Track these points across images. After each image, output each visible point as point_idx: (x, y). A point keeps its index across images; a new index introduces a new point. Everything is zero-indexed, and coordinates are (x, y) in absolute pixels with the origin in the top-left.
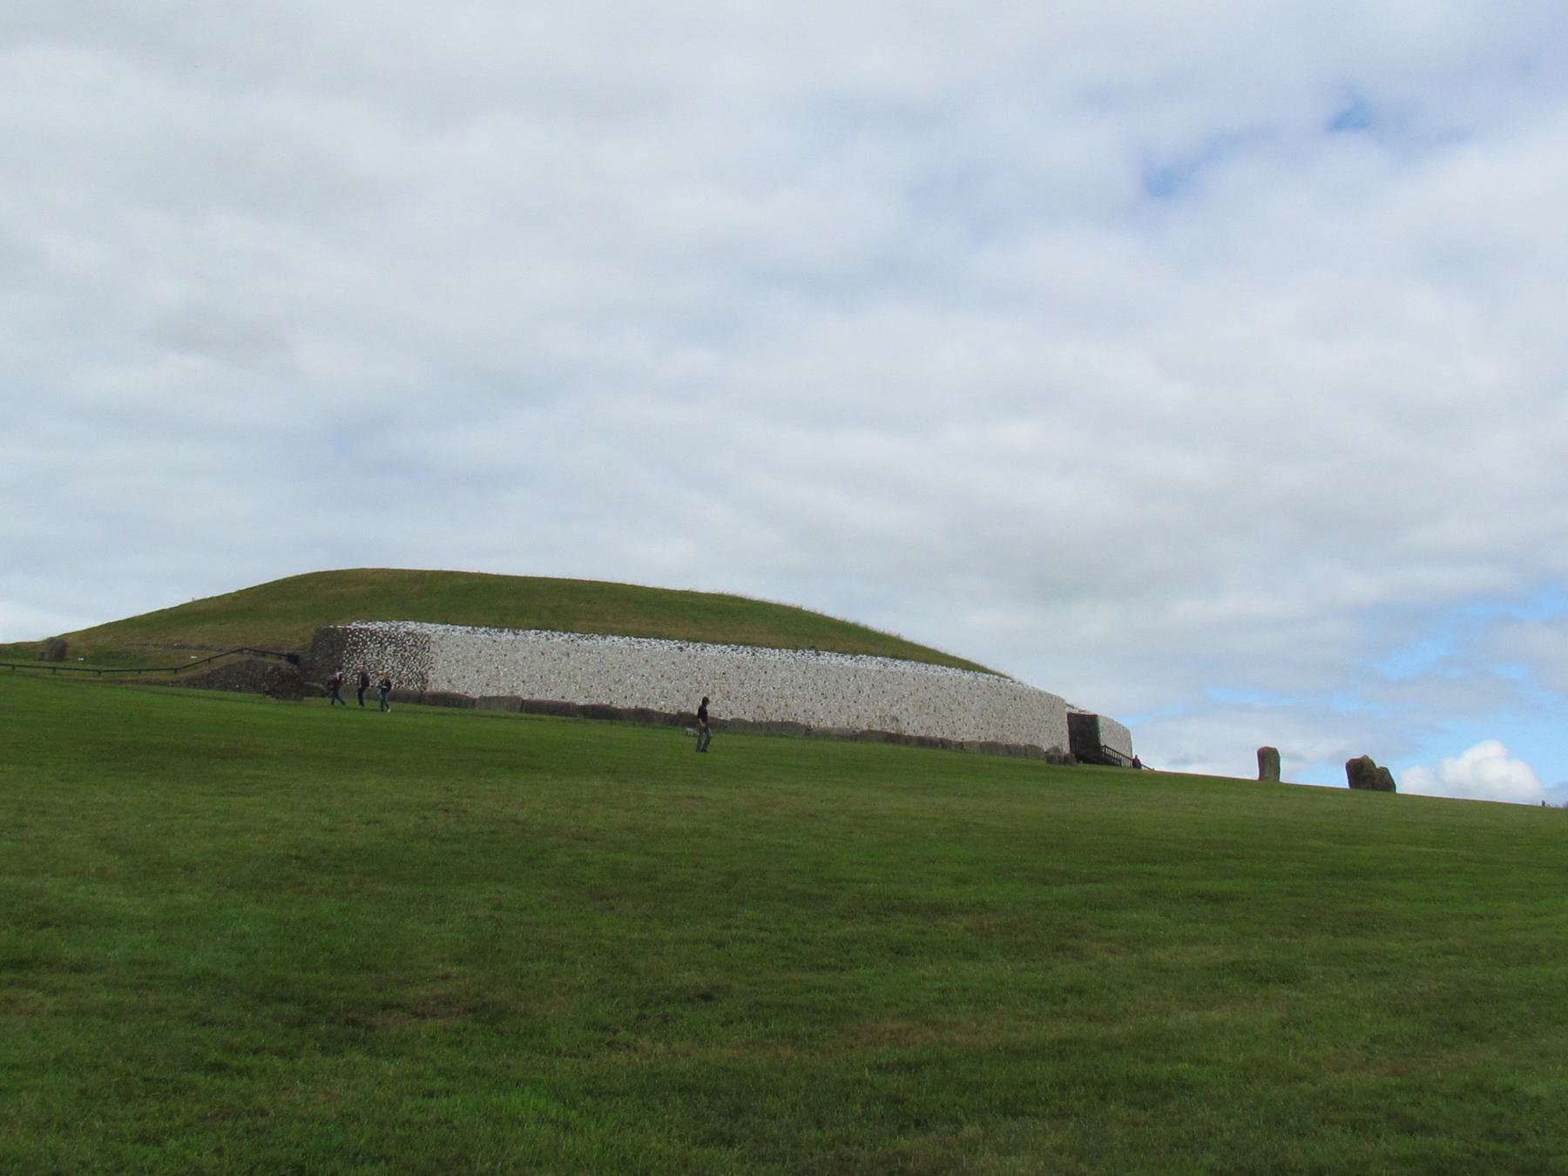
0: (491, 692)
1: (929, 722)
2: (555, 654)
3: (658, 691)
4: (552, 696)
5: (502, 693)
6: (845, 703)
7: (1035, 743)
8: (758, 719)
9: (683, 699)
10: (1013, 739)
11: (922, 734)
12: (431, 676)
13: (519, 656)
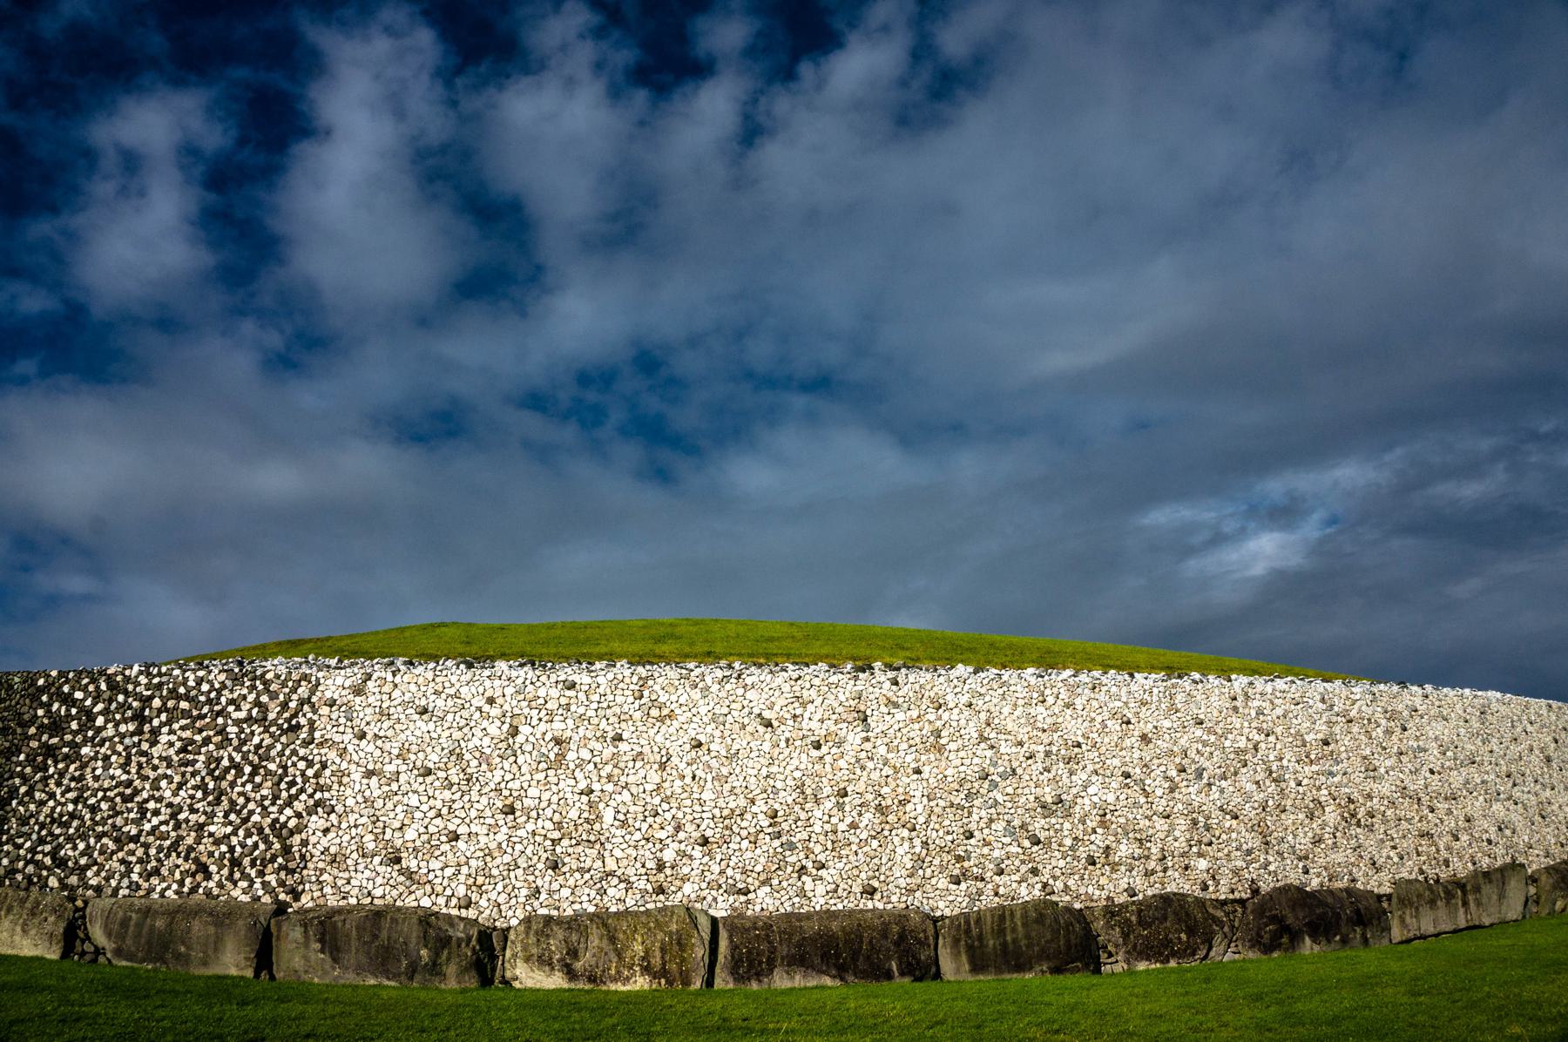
0: (572, 897)
2: (813, 724)
3: (1182, 824)
4: (824, 894)
5: (615, 898)
9: (1253, 841)
12: (318, 836)
13: (670, 736)
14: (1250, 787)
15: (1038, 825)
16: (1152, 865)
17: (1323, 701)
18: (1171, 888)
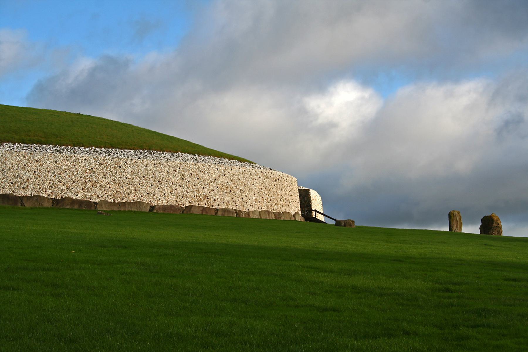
1: (228, 199)
3: (46, 183)
6: (174, 187)
7: (287, 210)
8: (117, 201)
10: (277, 209)
11: (224, 207)
14: (67, 177)
15: (13, 180)
16: (37, 190)
17: (94, 159)
18: (41, 195)
